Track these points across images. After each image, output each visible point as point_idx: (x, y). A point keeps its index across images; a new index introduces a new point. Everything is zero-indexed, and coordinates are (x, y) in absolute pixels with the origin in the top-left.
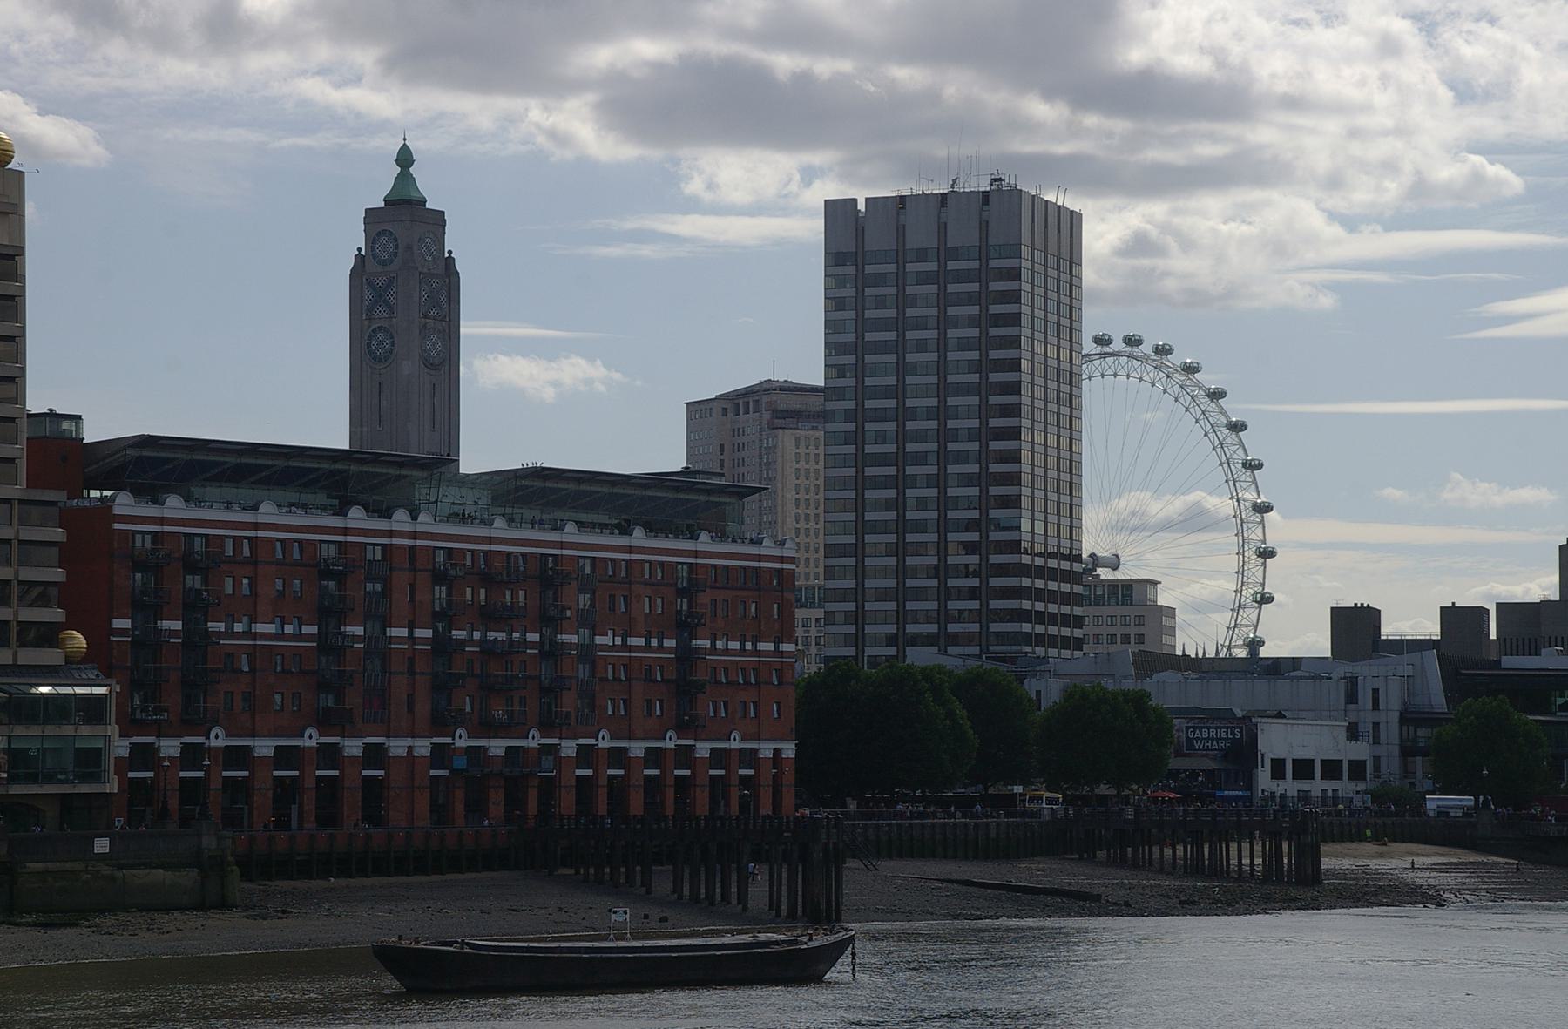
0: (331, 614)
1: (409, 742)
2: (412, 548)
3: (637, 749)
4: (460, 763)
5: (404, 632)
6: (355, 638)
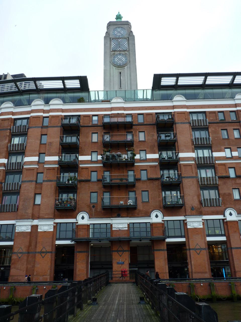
1: (36, 222)
5: (36, 159)
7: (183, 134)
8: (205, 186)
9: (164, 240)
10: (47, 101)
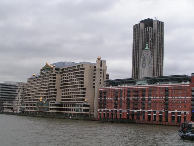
0: (117, 97)
1: (124, 110)
2: (125, 89)
3: (158, 112)
4: (130, 113)
6: (131, 99)
7: (147, 93)
8: (150, 104)
9: (141, 114)
10: (125, 85)
